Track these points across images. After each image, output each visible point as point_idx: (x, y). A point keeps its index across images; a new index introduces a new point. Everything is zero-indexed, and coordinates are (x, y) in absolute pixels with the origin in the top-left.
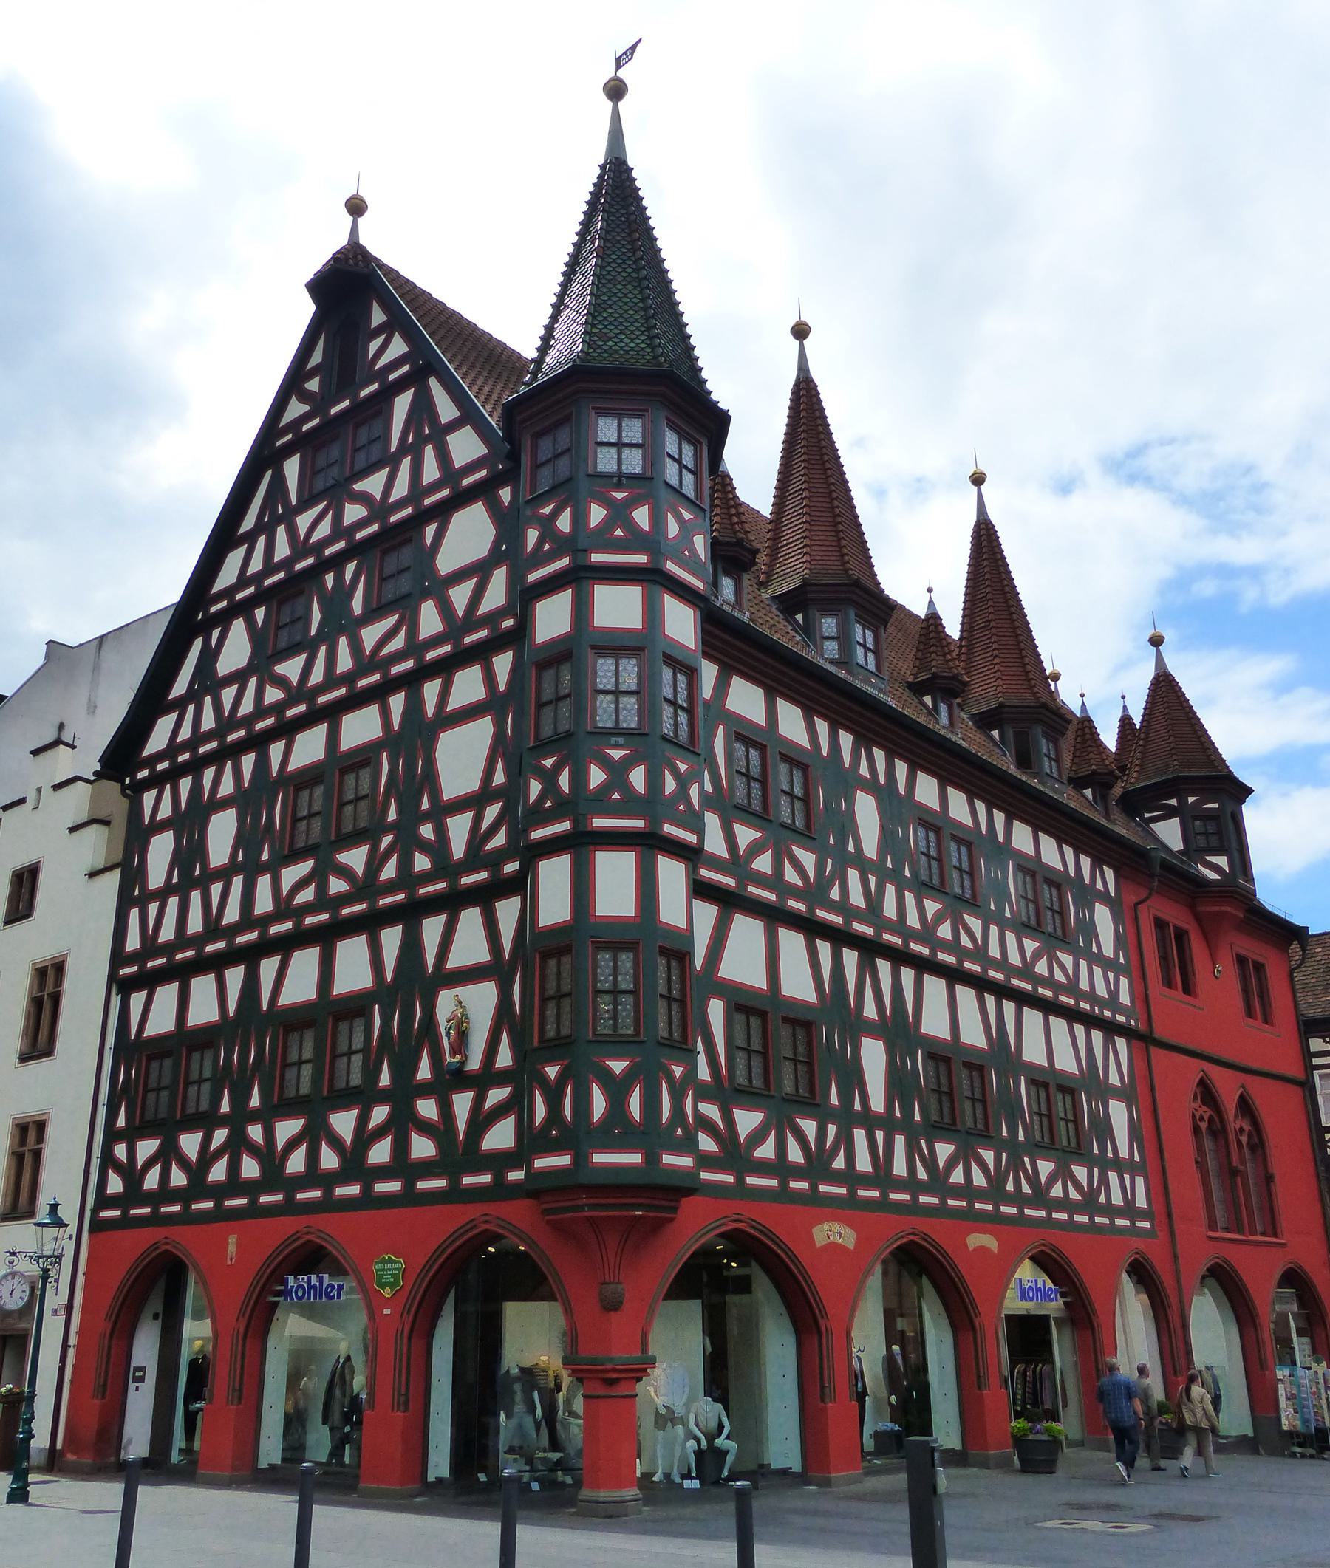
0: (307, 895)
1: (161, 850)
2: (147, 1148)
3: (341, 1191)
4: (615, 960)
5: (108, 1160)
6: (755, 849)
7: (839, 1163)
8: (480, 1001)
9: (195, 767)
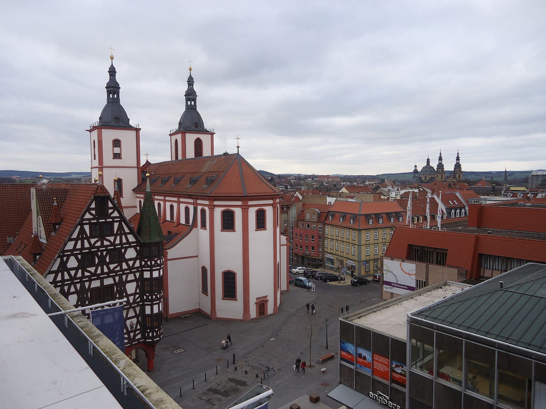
8: (135, 320)
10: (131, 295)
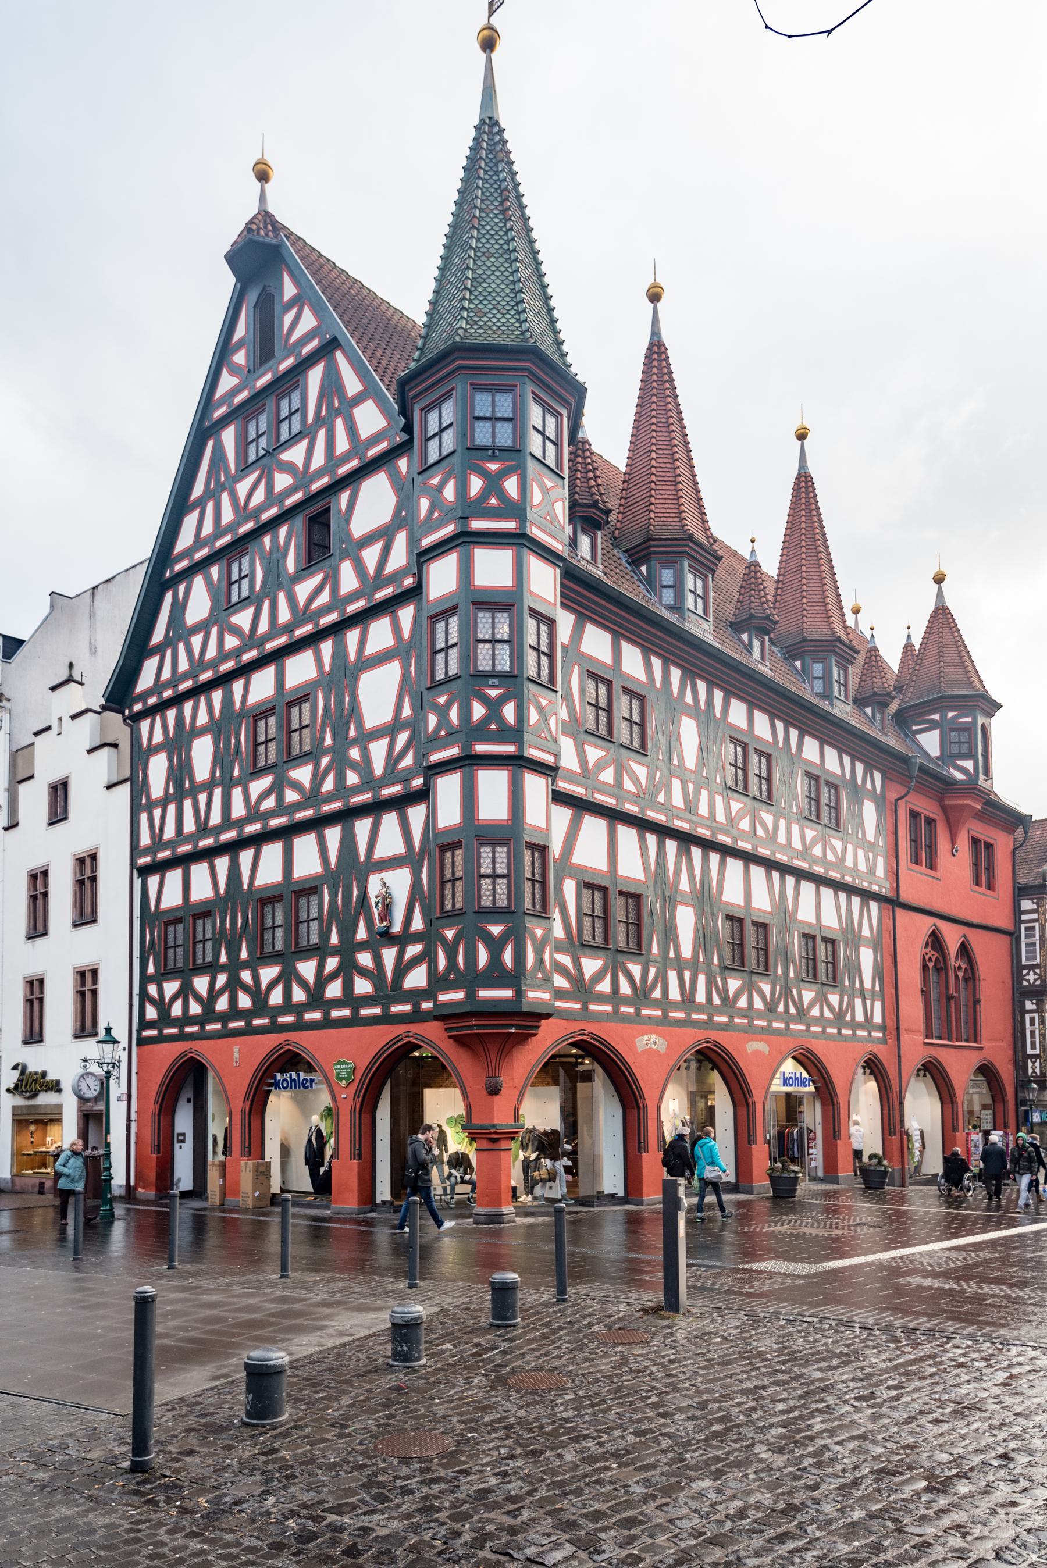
0: (269, 803)
3: (309, 1016)
4: (494, 852)
5: (144, 996)
6: (600, 766)
7: (657, 994)
9: (177, 700)
10: (376, 734)
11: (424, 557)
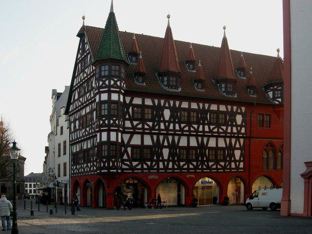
1: (72, 125)
2: (85, 165)
11: (95, 95)
